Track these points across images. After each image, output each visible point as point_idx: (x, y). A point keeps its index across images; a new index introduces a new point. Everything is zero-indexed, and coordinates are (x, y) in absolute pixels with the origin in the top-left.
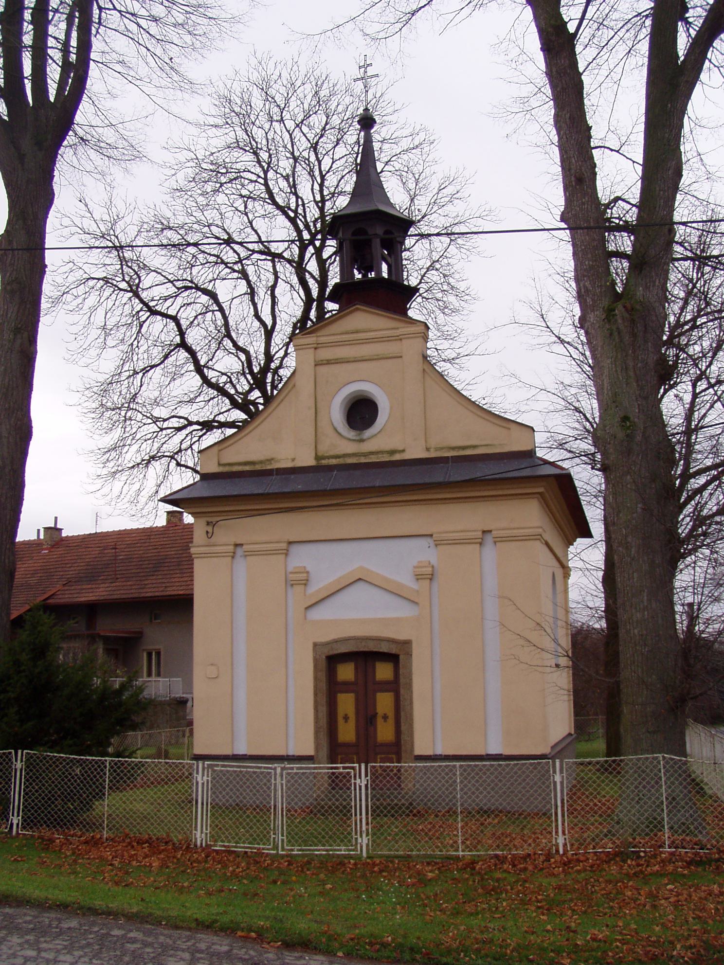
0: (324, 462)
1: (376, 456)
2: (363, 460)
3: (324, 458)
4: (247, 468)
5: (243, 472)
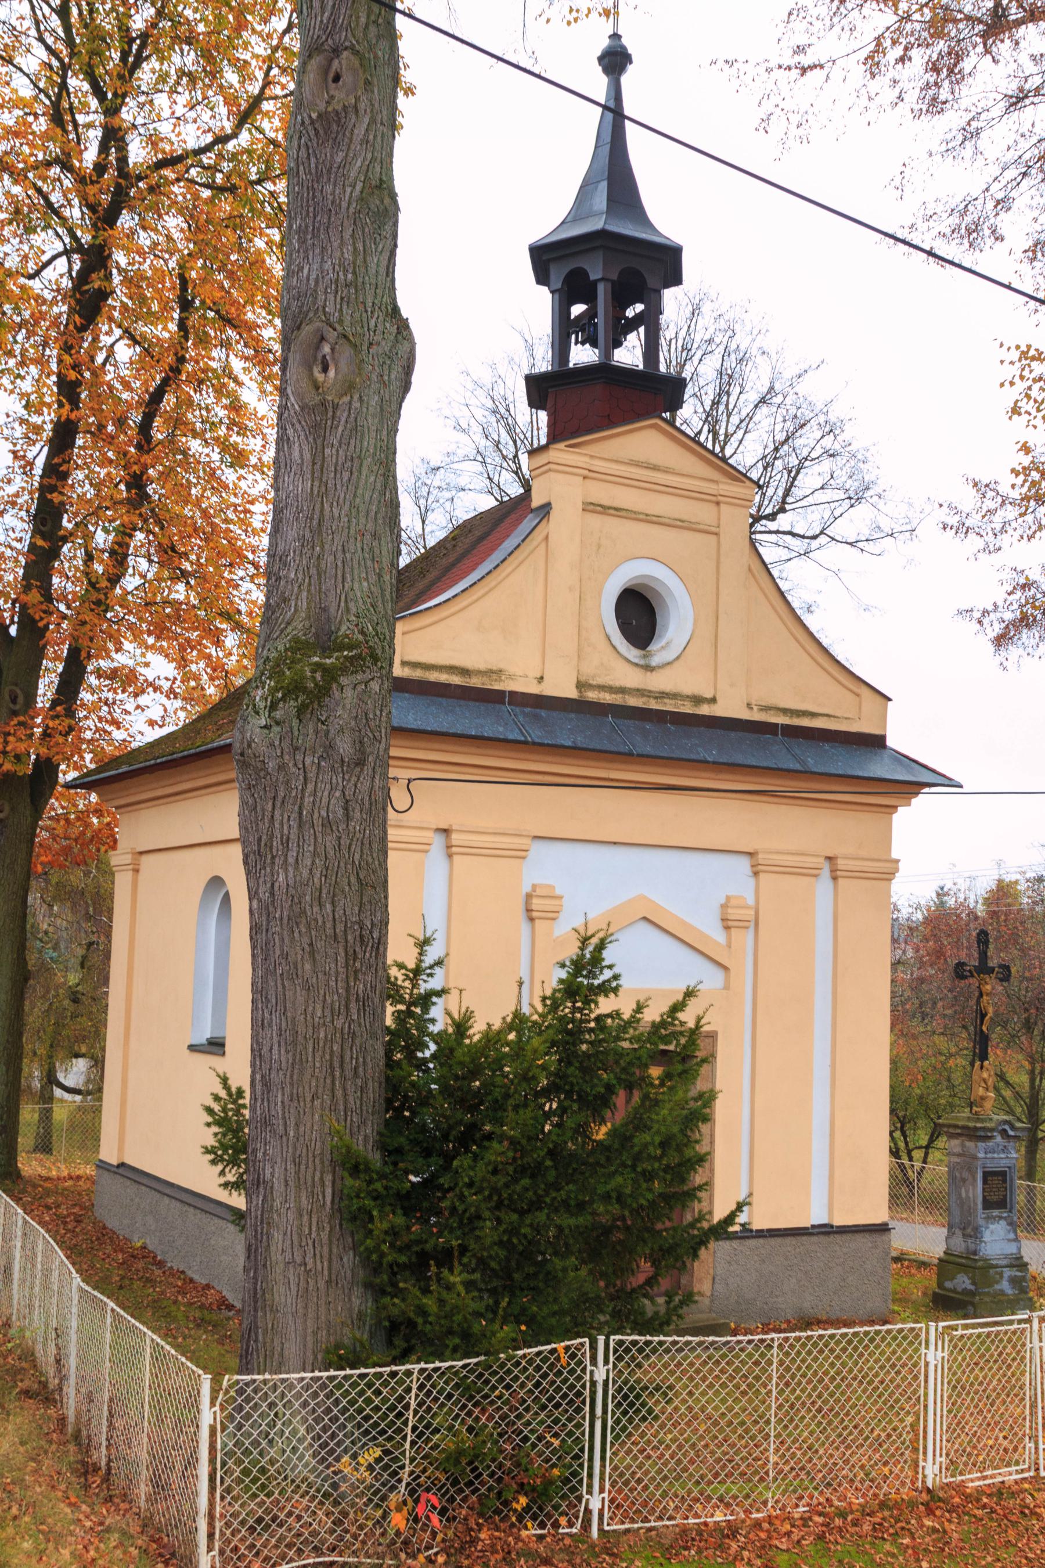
0: (592, 695)
1: (673, 702)
2: (653, 705)
3: (591, 687)
4: (456, 680)
5: (448, 686)
